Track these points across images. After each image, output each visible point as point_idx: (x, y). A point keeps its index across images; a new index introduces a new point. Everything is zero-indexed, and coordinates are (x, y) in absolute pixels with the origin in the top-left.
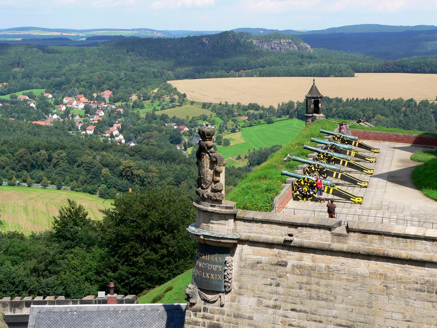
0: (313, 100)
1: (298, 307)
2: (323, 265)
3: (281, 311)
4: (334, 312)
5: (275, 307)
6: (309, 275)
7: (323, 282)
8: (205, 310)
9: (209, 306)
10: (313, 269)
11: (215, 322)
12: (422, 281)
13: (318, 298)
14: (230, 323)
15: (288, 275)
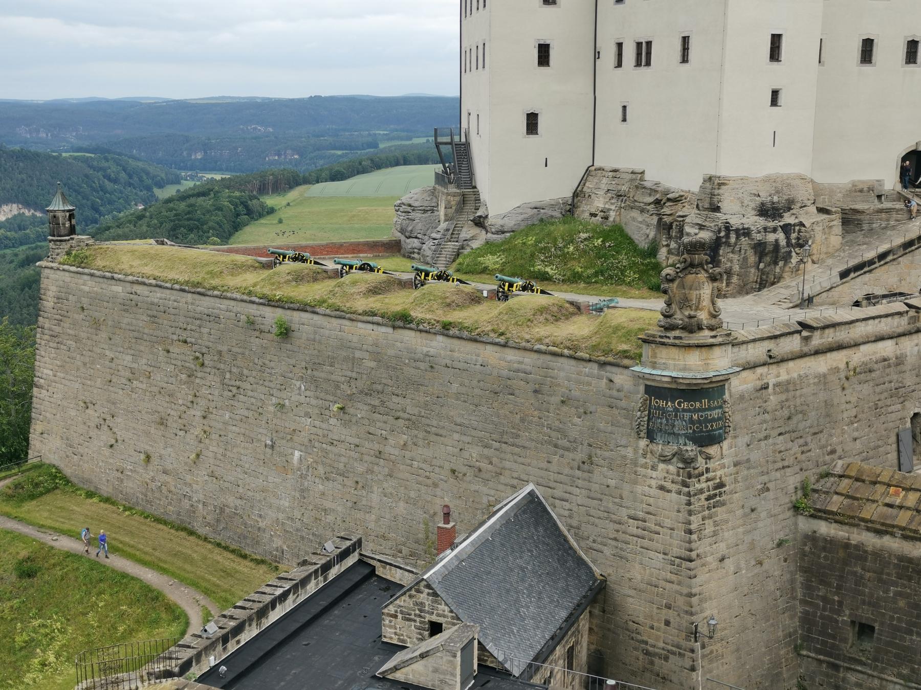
0: (68, 214)
1: (782, 430)
2: (795, 375)
3: (771, 441)
4: (808, 423)
5: (766, 438)
6: (787, 390)
7: (798, 393)
8: (708, 470)
9: (711, 465)
10: (788, 382)
11: (718, 481)
12: (860, 364)
13: (797, 413)
14: (731, 475)
15: (771, 397)
